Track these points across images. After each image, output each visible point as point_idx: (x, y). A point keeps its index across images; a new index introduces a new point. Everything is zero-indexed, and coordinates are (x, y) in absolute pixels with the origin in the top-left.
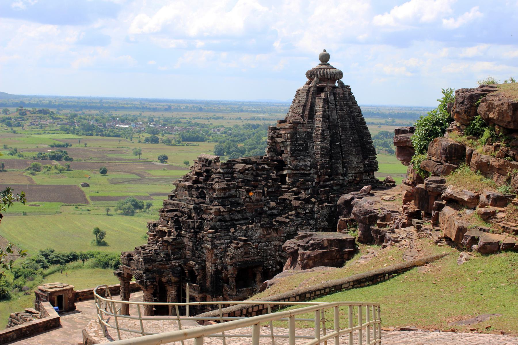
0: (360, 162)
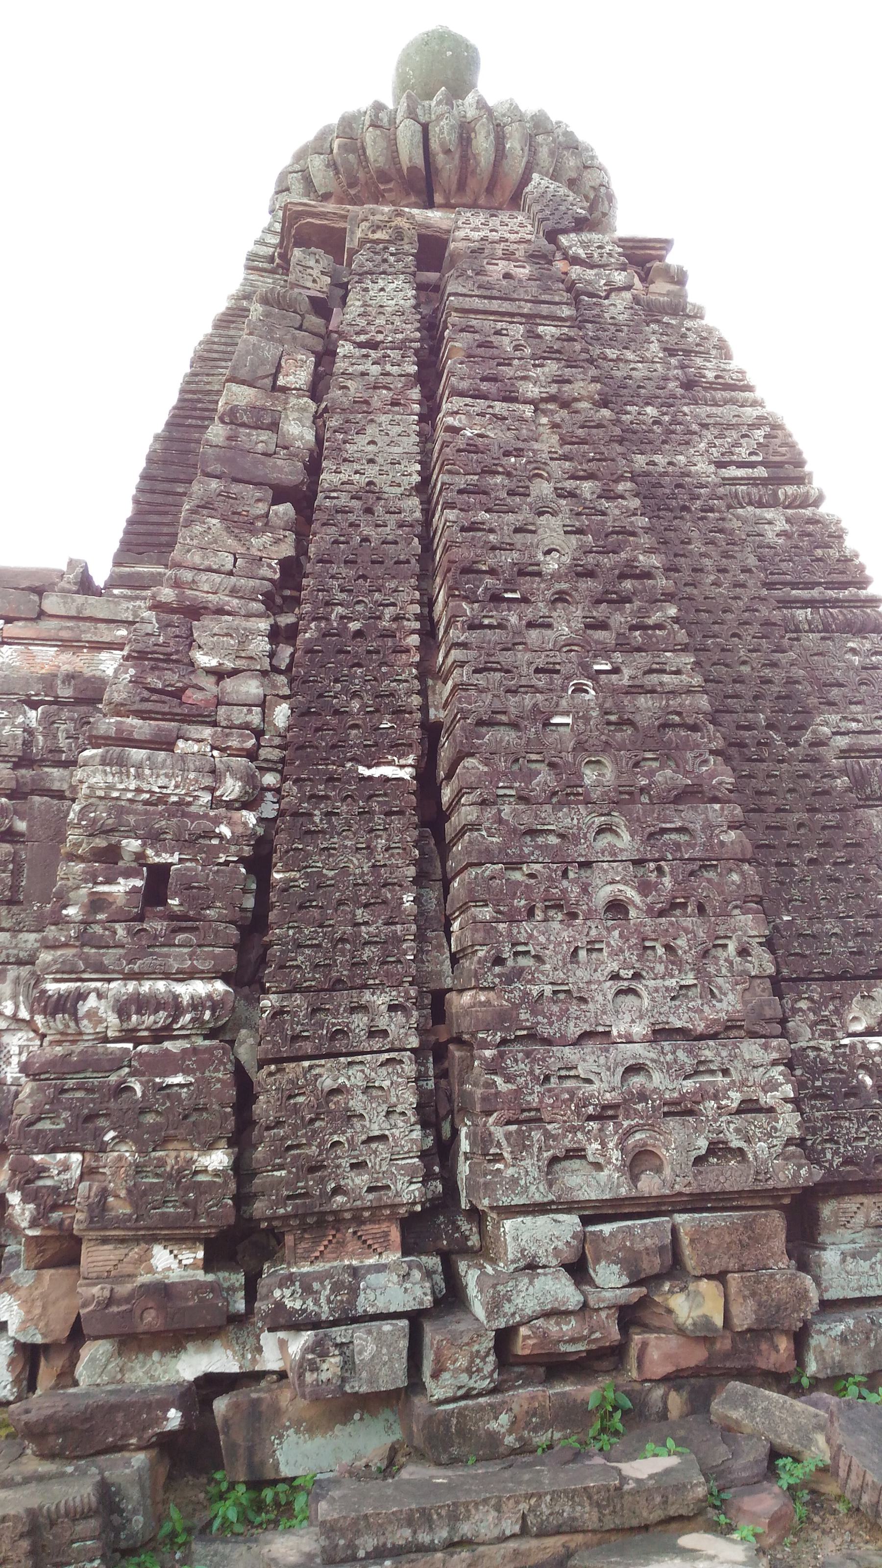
0: (725, 1031)
